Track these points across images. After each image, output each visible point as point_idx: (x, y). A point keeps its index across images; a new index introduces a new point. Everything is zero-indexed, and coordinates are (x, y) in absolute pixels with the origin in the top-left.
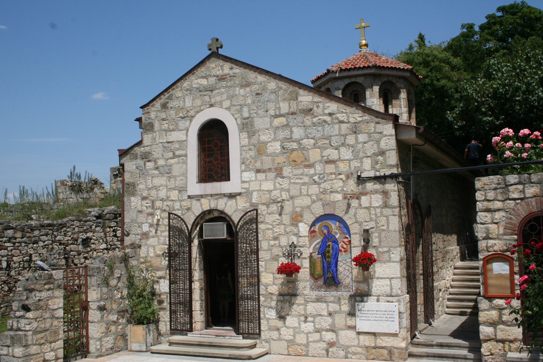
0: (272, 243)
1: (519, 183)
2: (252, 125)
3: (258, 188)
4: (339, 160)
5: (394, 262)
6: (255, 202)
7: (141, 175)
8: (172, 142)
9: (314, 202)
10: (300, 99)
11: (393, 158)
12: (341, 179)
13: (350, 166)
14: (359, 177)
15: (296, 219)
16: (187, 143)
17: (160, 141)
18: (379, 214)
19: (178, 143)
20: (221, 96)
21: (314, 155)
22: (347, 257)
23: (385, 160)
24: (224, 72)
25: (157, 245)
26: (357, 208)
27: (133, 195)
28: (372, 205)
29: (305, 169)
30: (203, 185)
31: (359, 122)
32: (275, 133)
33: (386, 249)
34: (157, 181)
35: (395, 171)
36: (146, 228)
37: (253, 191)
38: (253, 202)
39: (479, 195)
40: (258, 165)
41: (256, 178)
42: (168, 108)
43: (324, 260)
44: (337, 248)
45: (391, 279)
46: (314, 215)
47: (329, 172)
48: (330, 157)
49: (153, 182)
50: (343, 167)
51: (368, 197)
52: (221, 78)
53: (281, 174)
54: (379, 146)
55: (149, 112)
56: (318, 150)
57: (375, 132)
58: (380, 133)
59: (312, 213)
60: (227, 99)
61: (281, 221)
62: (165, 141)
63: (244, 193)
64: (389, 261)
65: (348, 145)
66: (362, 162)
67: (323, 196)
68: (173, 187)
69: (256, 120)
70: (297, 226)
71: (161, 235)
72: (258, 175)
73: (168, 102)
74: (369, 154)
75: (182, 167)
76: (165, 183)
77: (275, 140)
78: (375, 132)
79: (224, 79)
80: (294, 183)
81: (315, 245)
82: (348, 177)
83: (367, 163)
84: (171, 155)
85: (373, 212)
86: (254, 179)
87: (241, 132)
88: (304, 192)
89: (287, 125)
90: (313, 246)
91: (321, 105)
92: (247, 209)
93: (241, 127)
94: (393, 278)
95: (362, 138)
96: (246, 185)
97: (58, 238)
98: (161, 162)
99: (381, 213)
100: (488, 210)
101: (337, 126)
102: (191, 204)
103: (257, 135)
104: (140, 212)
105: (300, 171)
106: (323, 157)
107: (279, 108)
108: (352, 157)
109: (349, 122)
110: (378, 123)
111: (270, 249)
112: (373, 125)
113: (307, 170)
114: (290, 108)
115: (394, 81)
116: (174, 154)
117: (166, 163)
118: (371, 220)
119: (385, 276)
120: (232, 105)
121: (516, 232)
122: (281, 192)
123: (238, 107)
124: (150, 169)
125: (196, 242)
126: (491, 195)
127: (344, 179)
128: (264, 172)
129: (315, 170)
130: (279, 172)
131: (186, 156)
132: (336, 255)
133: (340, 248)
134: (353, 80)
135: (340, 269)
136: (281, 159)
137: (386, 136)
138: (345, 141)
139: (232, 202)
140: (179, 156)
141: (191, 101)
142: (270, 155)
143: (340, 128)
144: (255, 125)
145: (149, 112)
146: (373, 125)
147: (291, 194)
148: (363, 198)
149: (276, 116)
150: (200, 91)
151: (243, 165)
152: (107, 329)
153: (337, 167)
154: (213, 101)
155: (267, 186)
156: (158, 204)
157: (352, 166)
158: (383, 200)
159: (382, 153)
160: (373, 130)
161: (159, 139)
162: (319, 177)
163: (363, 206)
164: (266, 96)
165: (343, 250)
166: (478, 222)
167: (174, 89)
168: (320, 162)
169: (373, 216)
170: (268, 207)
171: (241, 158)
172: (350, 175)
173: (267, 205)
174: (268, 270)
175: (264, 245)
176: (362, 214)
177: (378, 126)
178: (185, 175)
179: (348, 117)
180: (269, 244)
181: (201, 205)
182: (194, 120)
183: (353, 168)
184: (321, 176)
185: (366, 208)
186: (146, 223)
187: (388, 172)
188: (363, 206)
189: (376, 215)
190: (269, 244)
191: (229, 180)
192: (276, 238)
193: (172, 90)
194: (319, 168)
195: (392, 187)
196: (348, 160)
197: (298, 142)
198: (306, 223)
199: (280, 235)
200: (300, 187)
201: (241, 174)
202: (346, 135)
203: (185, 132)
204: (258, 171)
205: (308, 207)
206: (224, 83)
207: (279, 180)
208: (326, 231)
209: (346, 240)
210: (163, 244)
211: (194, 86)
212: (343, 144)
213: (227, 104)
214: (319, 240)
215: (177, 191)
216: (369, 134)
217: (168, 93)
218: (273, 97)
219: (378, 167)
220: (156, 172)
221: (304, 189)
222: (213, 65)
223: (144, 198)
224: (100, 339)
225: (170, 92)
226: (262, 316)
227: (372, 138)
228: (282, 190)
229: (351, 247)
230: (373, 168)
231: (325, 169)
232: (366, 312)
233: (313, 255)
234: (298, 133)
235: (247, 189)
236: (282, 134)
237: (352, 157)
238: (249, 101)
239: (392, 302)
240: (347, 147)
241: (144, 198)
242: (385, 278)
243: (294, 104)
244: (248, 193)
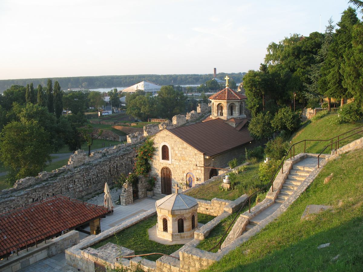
11: (203, 163)
15: (184, 172)
21: (187, 159)
30: (163, 160)
52: (167, 135)
72: (176, 161)
77: (179, 153)
95: (197, 157)
97: (129, 157)
110: (200, 154)
115: (234, 103)
134: (220, 103)
139: (169, 166)
146: (199, 155)
148: (197, 170)
152: (142, 193)
153: (192, 163)
154: (165, 140)
155: (177, 164)
164: (177, 142)
176: (197, 174)
177: (200, 155)
182: (161, 144)
191: (169, 160)
192: (179, 176)
195: (203, 169)
197: (184, 155)
204: (175, 160)
206: (167, 137)
213: (168, 142)
218: (178, 143)
219: (200, 164)
221: (185, 166)
222: (165, 132)
224: (141, 195)
230: (199, 164)
238: (173, 142)
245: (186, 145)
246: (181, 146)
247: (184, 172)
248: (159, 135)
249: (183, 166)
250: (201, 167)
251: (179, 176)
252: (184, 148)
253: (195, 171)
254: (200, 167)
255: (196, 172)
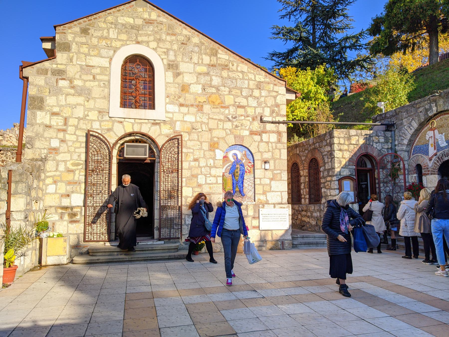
0: (193, 164)
1: (356, 135)
2: (177, 67)
3: (181, 119)
4: (248, 106)
5: (283, 180)
6: (178, 130)
7: (51, 91)
8: (92, 66)
9: (227, 135)
10: (219, 56)
12: (249, 120)
13: (255, 112)
14: (261, 119)
16: (110, 70)
17: (78, 63)
18: (274, 148)
19: (99, 68)
20: (148, 37)
21: (229, 100)
22: (251, 177)
23: (279, 111)
24: (151, 18)
25: (69, 161)
26: (259, 142)
27: (41, 108)
28: (270, 141)
29: (221, 109)
30: (127, 110)
31: (263, 82)
32: (197, 78)
33: (279, 172)
34: (72, 100)
35: (285, 119)
36: (55, 143)
37: (176, 121)
38: (176, 129)
39: (336, 140)
40: (181, 100)
41: (179, 110)
42: (89, 34)
43: (233, 178)
44: (243, 170)
45: (281, 192)
46: (228, 144)
47: (239, 114)
48: (241, 104)
49: (68, 100)
50: (250, 111)
51: (268, 134)
52: (149, 22)
53: (202, 110)
54: (275, 100)
55: (65, 33)
56: (232, 97)
57: (273, 91)
58: (277, 92)
59: (226, 143)
60: (153, 41)
61: (202, 147)
62: (84, 64)
63: (168, 121)
64: (281, 180)
65: (254, 96)
66: (263, 110)
67: (235, 131)
68: (92, 107)
69: (181, 64)
70: (214, 151)
71: (75, 152)
73: (89, 29)
74: (269, 105)
75: (103, 90)
76: (82, 103)
77: (197, 83)
78: (273, 91)
79: (151, 23)
80: (212, 119)
81: (227, 167)
82: (253, 119)
83: (267, 112)
84: (91, 77)
85: (270, 145)
86: (178, 111)
87: (167, 71)
88: (221, 127)
89: (207, 74)
90: (225, 167)
91: (235, 64)
92: (171, 134)
93: (167, 67)
94: (283, 191)
95: (264, 93)
96: (170, 115)
98: (77, 83)
99: (276, 146)
100: (340, 150)
101: (246, 82)
102: (113, 125)
103: (181, 76)
104: (49, 127)
105: (217, 110)
106: (236, 102)
107: (202, 59)
108: (257, 106)
109: (255, 80)
111: (190, 168)
112: (272, 85)
113: (223, 110)
114: (211, 60)
116: (94, 77)
117: (84, 84)
118: (269, 151)
119: (278, 190)
120: (158, 47)
121: (355, 164)
122: (201, 125)
123: (165, 50)
124: (65, 88)
125: (115, 161)
126: (342, 141)
127: (251, 120)
128: (187, 106)
129: (229, 111)
130: (200, 107)
131: (109, 81)
132: (242, 175)
133: (246, 170)
135: (245, 185)
136: (202, 99)
137: (280, 94)
138: (252, 93)
140: (101, 80)
141: (116, 35)
142: (192, 94)
143: (249, 83)
144: (180, 68)
145: (65, 33)
146: (272, 85)
147: (210, 127)
148: (264, 135)
149: (198, 64)
150: (126, 28)
151: (168, 99)
154: (140, 39)
155: (190, 118)
156: (72, 121)
157: (256, 112)
158: (277, 138)
159: (278, 106)
160: (272, 89)
161: (77, 60)
162: (232, 117)
163: (264, 141)
164: (190, 48)
165: (248, 171)
166: (336, 156)
167: (96, 18)
168: (234, 105)
169: (271, 148)
170: (189, 135)
171: (166, 93)
172: (255, 118)
173: (189, 133)
174: (188, 185)
175: (185, 165)
177: (275, 87)
178: (108, 98)
179: (255, 77)
180: (190, 164)
181: (124, 127)
182: (118, 53)
183: (257, 113)
184: (234, 116)
185: (266, 142)
186: (55, 138)
187: (281, 119)
188: (264, 141)
189: (272, 147)
190: (190, 164)
192: (196, 160)
193: (94, 19)
194: (232, 109)
196: (254, 107)
198: (221, 150)
199: (200, 158)
200: (218, 122)
201: (166, 106)
202: (253, 89)
203: (108, 60)
204: (181, 105)
205: (223, 138)
206: (151, 28)
207: (200, 114)
208: (235, 157)
209: (250, 164)
210: (77, 160)
211: (120, 21)
212: (251, 95)
213: (153, 45)
214: (230, 163)
215: (97, 112)
216: (269, 91)
217: (89, 20)
218: (196, 49)
220: (72, 91)
222: (140, 10)
223: (54, 114)
225: (91, 20)
226: (183, 222)
227: (271, 94)
228: (202, 123)
229: (254, 169)
230: (271, 115)
231: (236, 111)
232: (267, 215)
233: (225, 174)
234: (216, 81)
235: (171, 119)
236: (203, 80)
237: (257, 106)
238: (175, 47)
239: (284, 208)
240: (254, 98)
241: (54, 114)
242: (278, 192)
243: (214, 59)
244: (172, 123)
245: (227, 57)
246: (206, 59)
247: (218, 143)
248: (110, 18)
249: (212, 124)
250: (279, 123)
251: (196, 160)
252: (220, 65)
253: (257, 138)
254: (273, 123)
255: (262, 140)
